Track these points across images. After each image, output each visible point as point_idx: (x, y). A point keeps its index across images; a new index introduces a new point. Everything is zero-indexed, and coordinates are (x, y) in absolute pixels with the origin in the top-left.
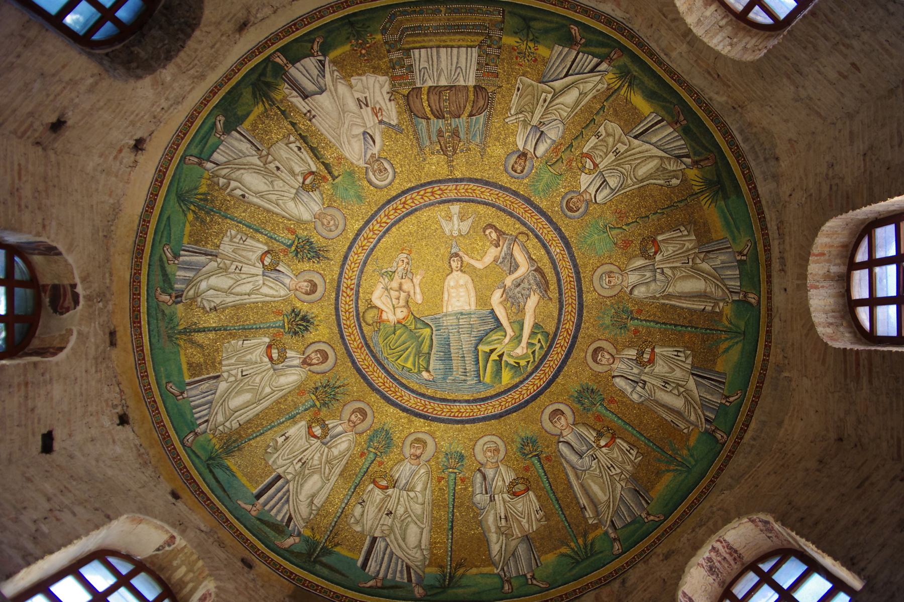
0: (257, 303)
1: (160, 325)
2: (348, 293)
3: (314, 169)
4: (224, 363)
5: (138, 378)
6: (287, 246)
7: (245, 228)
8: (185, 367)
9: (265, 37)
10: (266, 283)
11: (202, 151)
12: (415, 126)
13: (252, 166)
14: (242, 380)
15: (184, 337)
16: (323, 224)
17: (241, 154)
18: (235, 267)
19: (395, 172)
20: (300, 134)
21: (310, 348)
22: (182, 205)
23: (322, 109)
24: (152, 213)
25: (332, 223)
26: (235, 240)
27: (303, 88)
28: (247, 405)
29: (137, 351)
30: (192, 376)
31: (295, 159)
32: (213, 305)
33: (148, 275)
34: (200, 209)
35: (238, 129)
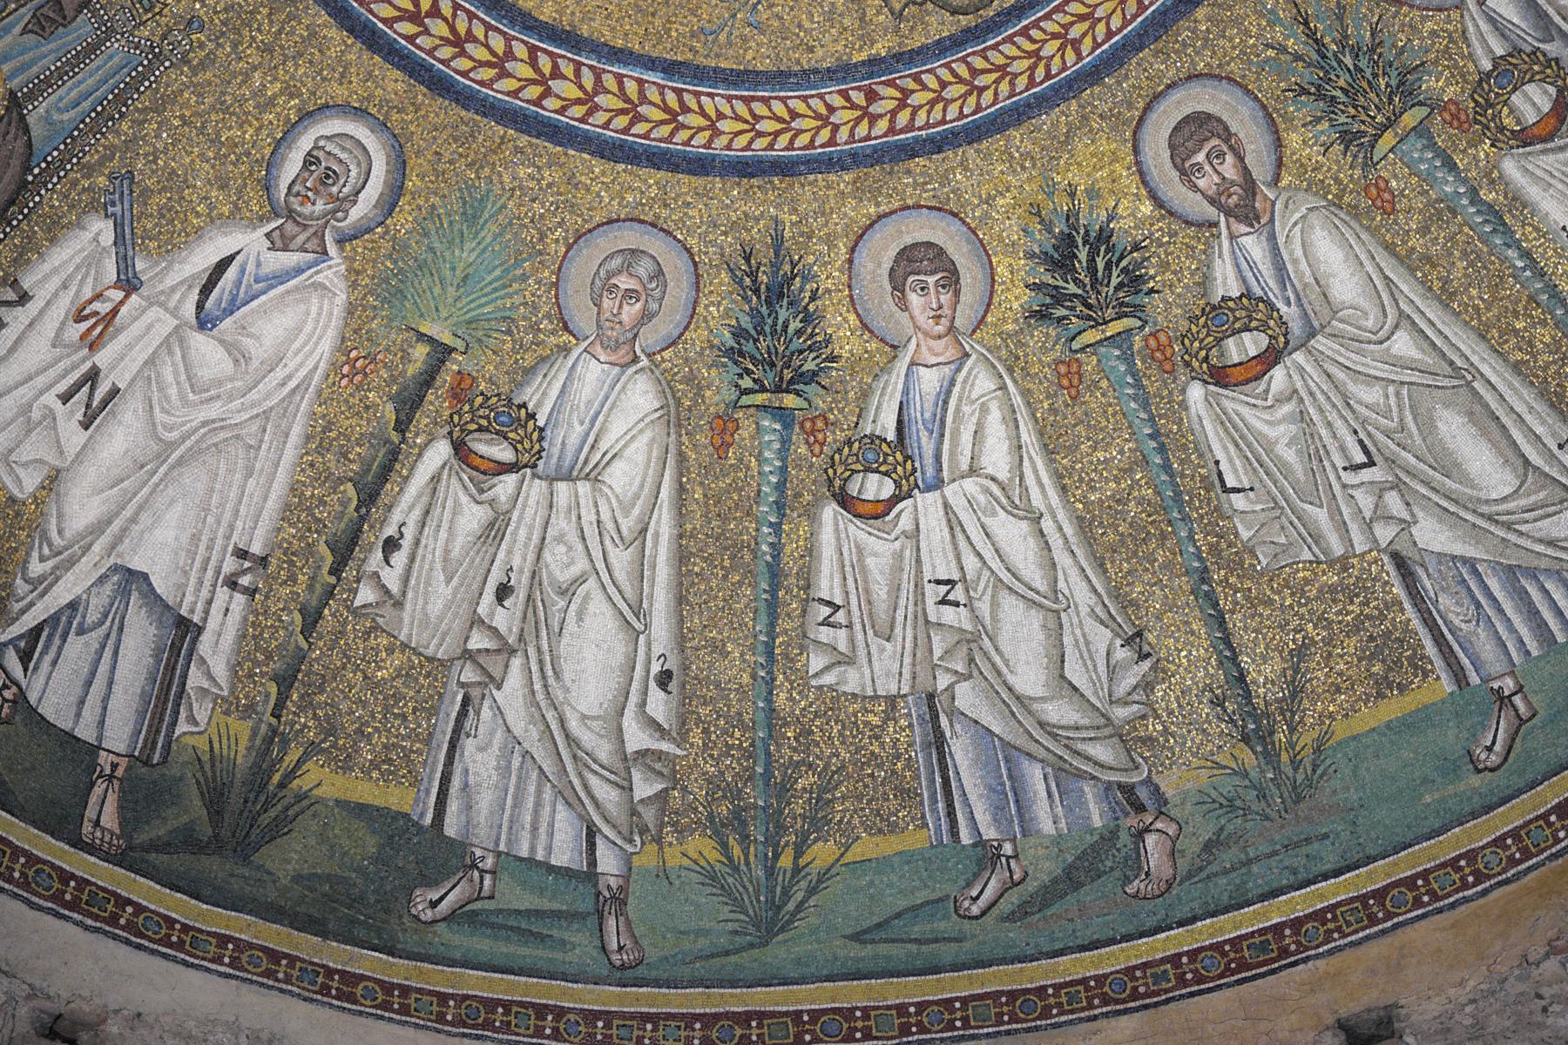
0: (1058, 476)
1: (1264, 848)
2: (892, 104)
3: (440, 451)
4: (1338, 550)
5: (1485, 893)
6: (787, 426)
7: (783, 624)
8: (1393, 708)
9: (59, 923)
10: (965, 467)
11: (573, 916)
12: (74, 141)
13: (540, 696)
14: (1391, 462)
15: (1281, 737)
16: (646, 316)
17: (516, 762)
18: (948, 611)
19: (307, 116)
20: (336, 571)
21: (1176, 205)
22: (791, 906)
23: (195, 538)
24: (865, 1010)
25: (624, 282)
26: (843, 646)
27: (157, 656)
28: (1488, 423)
29: (1389, 916)
30: (1420, 666)
31: (434, 545)
32: (1121, 654)
33: (1095, 945)
34: (781, 828)
35: (428, 819)
